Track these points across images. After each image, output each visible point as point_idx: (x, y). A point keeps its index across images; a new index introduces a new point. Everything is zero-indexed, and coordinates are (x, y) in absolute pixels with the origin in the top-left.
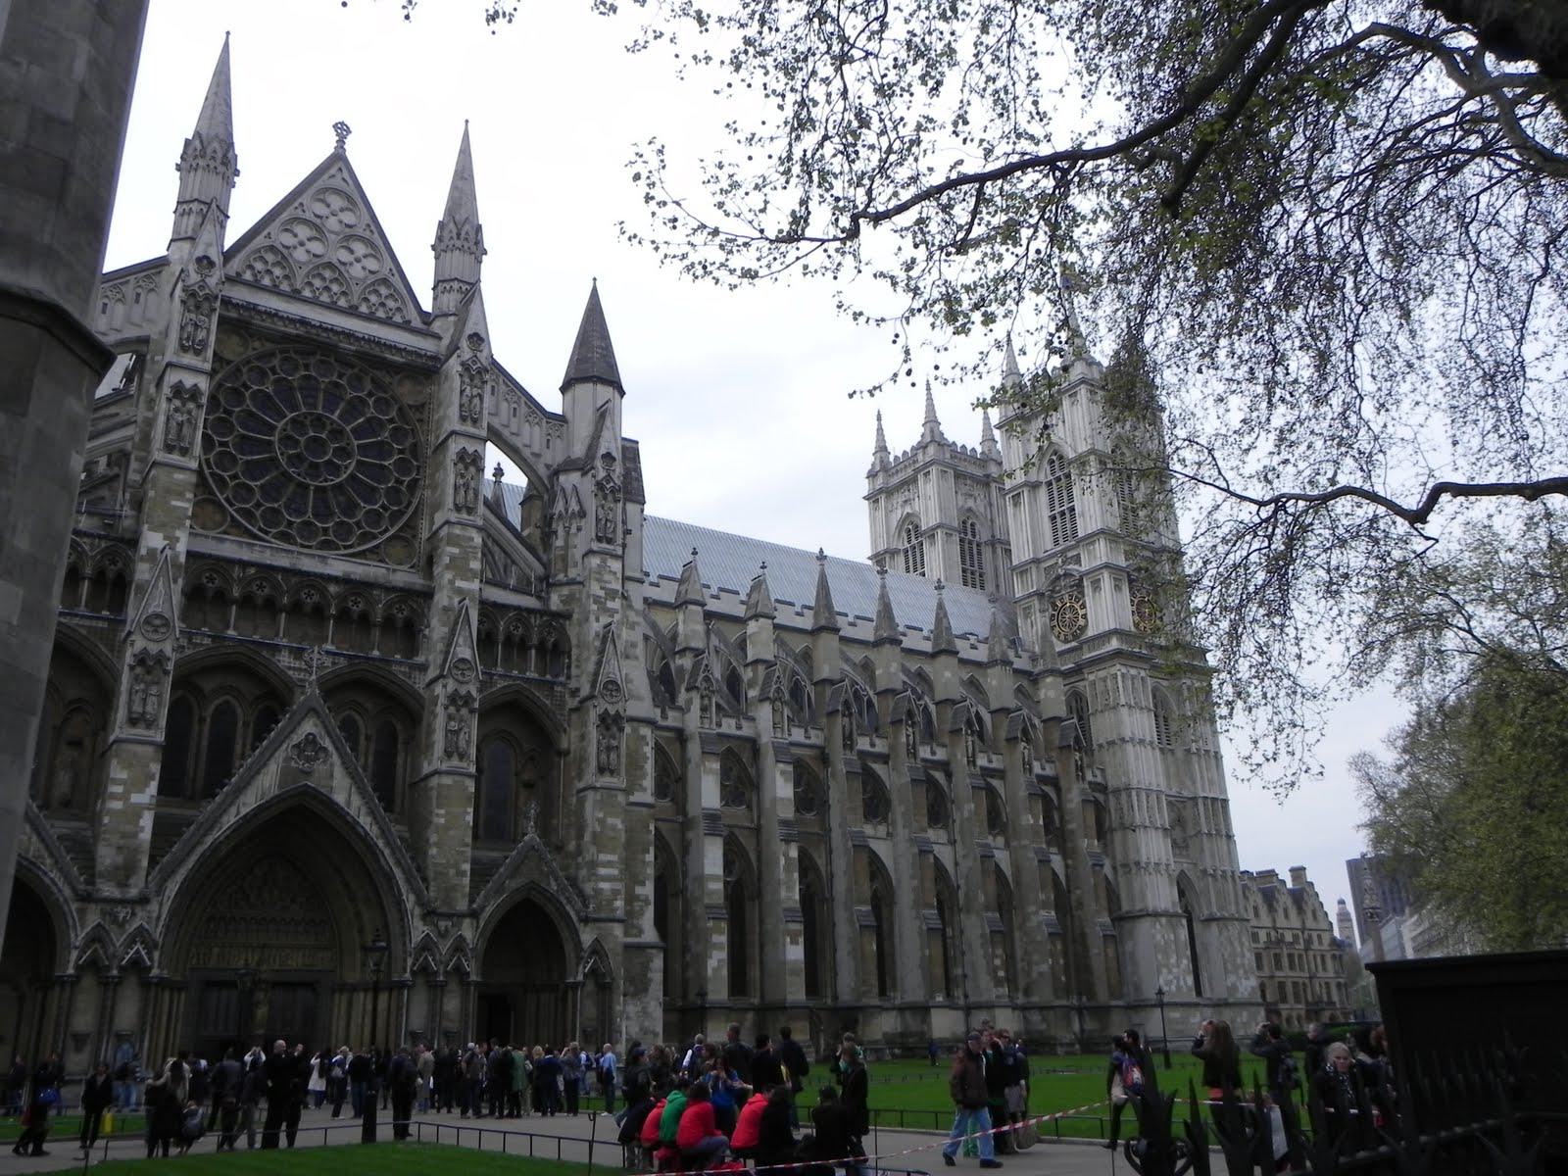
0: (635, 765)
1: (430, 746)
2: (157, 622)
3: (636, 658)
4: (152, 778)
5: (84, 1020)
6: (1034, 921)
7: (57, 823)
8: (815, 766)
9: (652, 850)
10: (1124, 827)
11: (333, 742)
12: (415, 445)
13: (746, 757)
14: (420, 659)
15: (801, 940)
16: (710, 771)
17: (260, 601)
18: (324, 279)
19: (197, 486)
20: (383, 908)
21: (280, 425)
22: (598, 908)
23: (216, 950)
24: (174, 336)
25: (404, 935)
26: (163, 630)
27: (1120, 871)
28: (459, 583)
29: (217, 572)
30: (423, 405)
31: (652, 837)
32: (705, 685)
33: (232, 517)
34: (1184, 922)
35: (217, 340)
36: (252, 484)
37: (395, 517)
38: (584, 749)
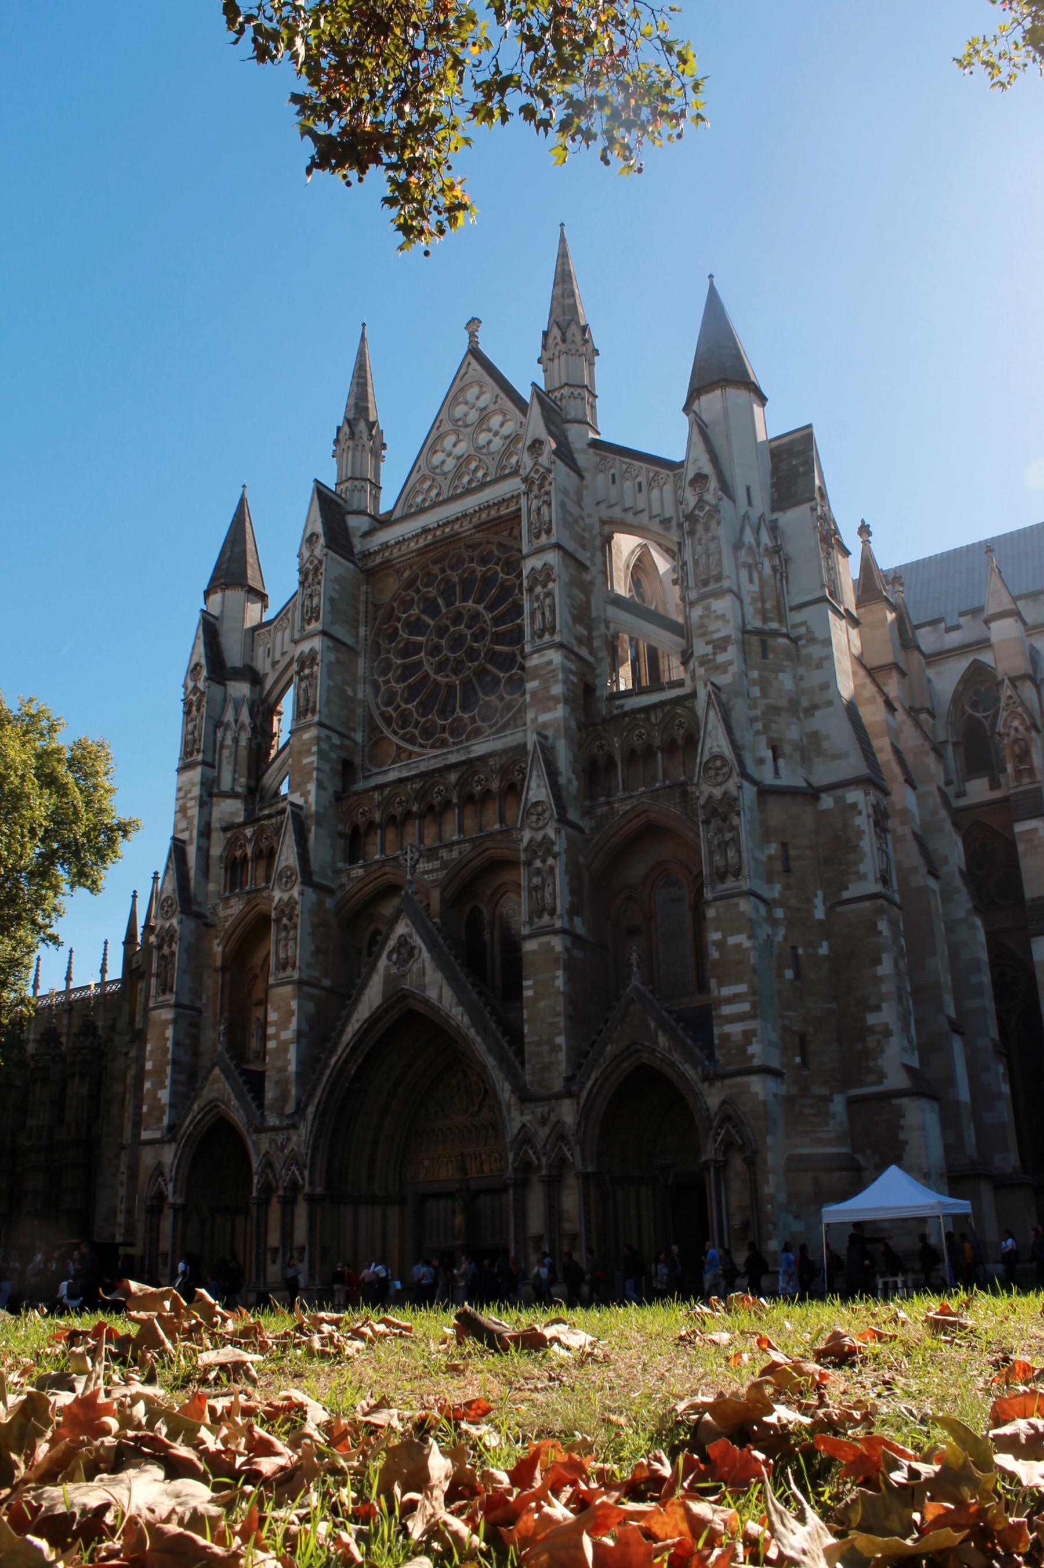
2: (289, 873)
28: (543, 718)
33: (397, 745)
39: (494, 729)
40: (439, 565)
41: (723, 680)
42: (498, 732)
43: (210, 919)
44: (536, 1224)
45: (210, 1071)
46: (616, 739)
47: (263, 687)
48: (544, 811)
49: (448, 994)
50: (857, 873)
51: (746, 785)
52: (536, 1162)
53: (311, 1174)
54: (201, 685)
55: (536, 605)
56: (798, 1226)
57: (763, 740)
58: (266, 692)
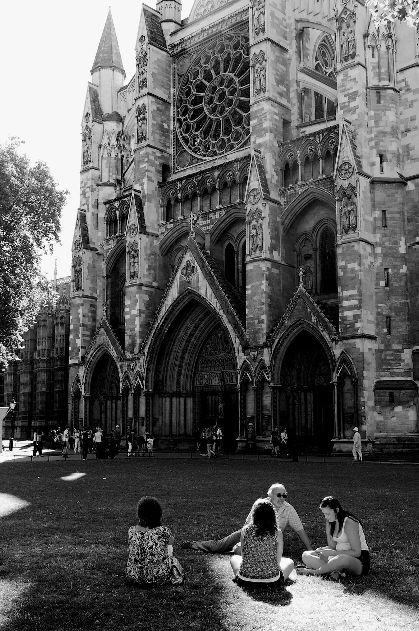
5: (130, 414)
28: (259, 141)
33: (191, 155)
36: (197, 133)
40: (211, 51)
41: (351, 117)
42: (242, 146)
43: (100, 251)
44: (251, 410)
45: (99, 329)
46: (298, 152)
47: (123, 124)
48: (257, 194)
49: (210, 291)
51: (362, 178)
52: (251, 380)
53: (146, 382)
54: (90, 125)
55: (256, 75)
56: (380, 418)
57: (375, 152)
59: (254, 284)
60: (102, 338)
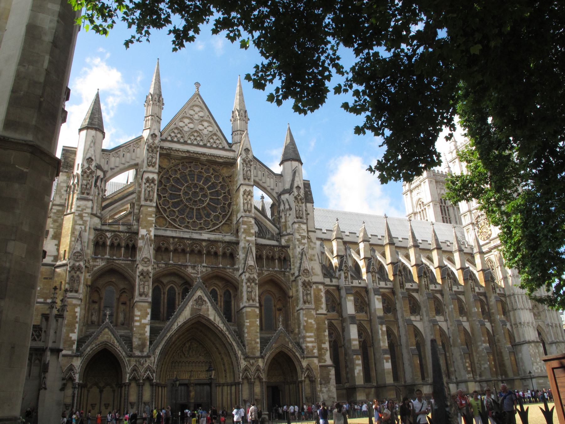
0: (318, 300)
1: (242, 298)
2: (146, 260)
3: (315, 260)
4: (148, 314)
5: (133, 398)
6: (481, 348)
7: (119, 331)
8: (390, 296)
9: (327, 331)
10: (514, 310)
11: (208, 299)
12: (229, 190)
13: (363, 294)
14: (236, 267)
15: (390, 361)
16: (350, 300)
17: (180, 250)
18: (194, 136)
19: (157, 212)
20: (230, 355)
21: (183, 188)
22: (308, 352)
23: (175, 373)
24: (145, 162)
25: (238, 366)
26: (148, 263)
27: (513, 326)
28: (248, 238)
29: (165, 241)
30: (231, 176)
31: (327, 326)
32: (345, 268)
33: (169, 222)
34: (541, 344)
35: (160, 161)
36: (175, 210)
37: (224, 216)
38: (298, 295)
39: (209, 230)
42: (211, 231)
43: (87, 264)
50: (321, 307)
53: (156, 375)
55: (245, 201)
58: (106, 178)
59: (251, 320)
60: (106, 336)
